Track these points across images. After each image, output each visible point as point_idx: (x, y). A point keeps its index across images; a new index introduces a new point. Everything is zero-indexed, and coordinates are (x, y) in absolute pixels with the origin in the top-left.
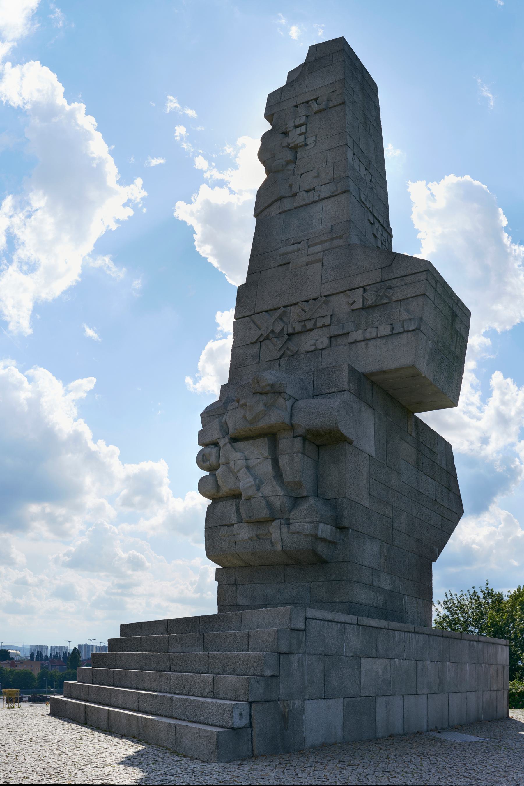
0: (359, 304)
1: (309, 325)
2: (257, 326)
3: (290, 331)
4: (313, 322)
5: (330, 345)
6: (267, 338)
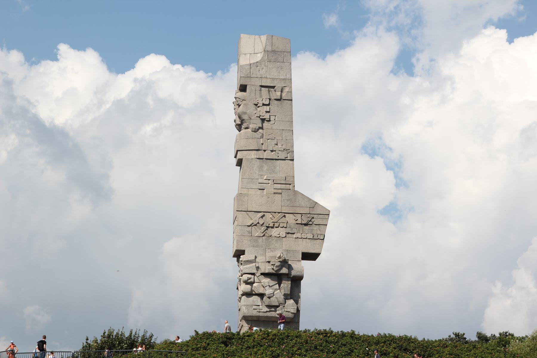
0: (299, 221)
3: (267, 225)
5: (286, 237)
6: (256, 225)
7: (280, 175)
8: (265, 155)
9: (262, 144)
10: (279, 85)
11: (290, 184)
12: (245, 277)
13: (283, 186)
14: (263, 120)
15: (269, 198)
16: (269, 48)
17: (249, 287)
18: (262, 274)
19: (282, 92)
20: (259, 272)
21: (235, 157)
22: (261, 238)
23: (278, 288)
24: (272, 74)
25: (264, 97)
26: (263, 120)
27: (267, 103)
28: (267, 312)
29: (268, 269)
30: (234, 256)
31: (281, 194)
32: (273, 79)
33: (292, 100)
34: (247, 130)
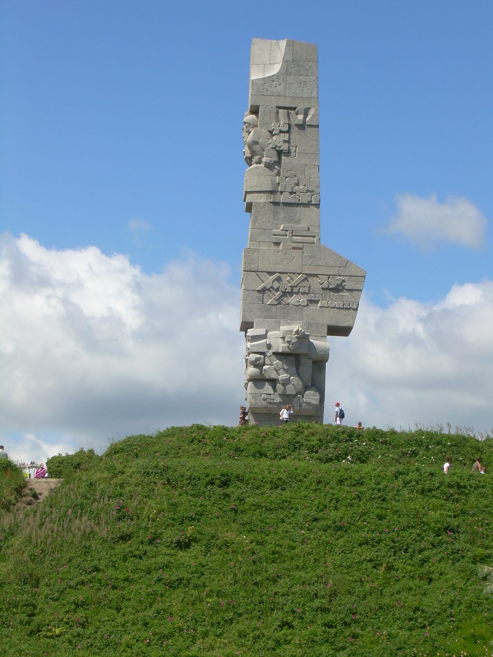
1: (295, 290)
2: (261, 280)
4: (298, 288)
5: (308, 305)
8: (282, 199)
9: (279, 184)
10: (301, 107)
11: (314, 237)
12: (253, 357)
14: (280, 153)
15: (286, 254)
16: (290, 58)
17: (257, 370)
18: (274, 354)
19: (306, 115)
20: (271, 351)
21: (245, 200)
24: (293, 91)
25: (282, 123)
26: (280, 153)
27: (286, 128)
30: (241, 330)
31: (301, 249)
32: (294, 98)
33: (317, 126)
34: (258, 165)
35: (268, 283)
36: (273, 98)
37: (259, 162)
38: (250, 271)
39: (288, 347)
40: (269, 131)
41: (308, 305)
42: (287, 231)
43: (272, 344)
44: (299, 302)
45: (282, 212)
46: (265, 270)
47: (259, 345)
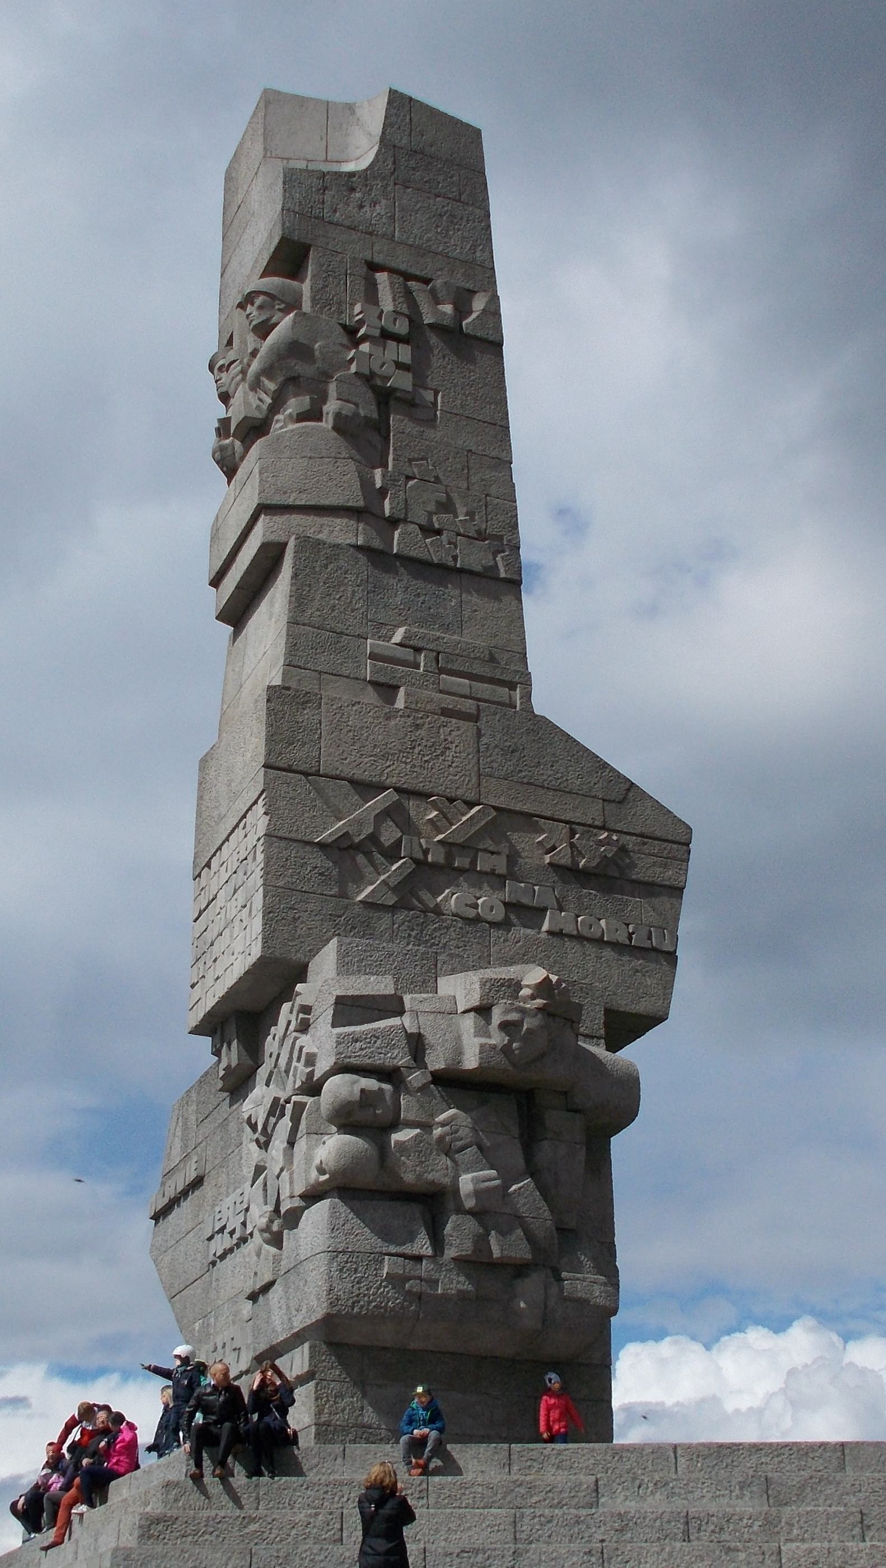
6: (357, 848)
7: (472, 638)
13: (483, 689)
22: (386, 919)
23: (520, 1162)
28: (462, 1295)
29: (471, 1048)
32: (421, 251)
35: (360, 822)
36: (355, 236)
37: (313, 414)
38: (289, 770)
39: (506, 1050)
40: (344, 327)
41: (505, 924)
42: (418, 650)
43: (430, 1038)
44: (475, 906)
45: (399, 588)
46: (347, 771)
47: (375, 1036)
